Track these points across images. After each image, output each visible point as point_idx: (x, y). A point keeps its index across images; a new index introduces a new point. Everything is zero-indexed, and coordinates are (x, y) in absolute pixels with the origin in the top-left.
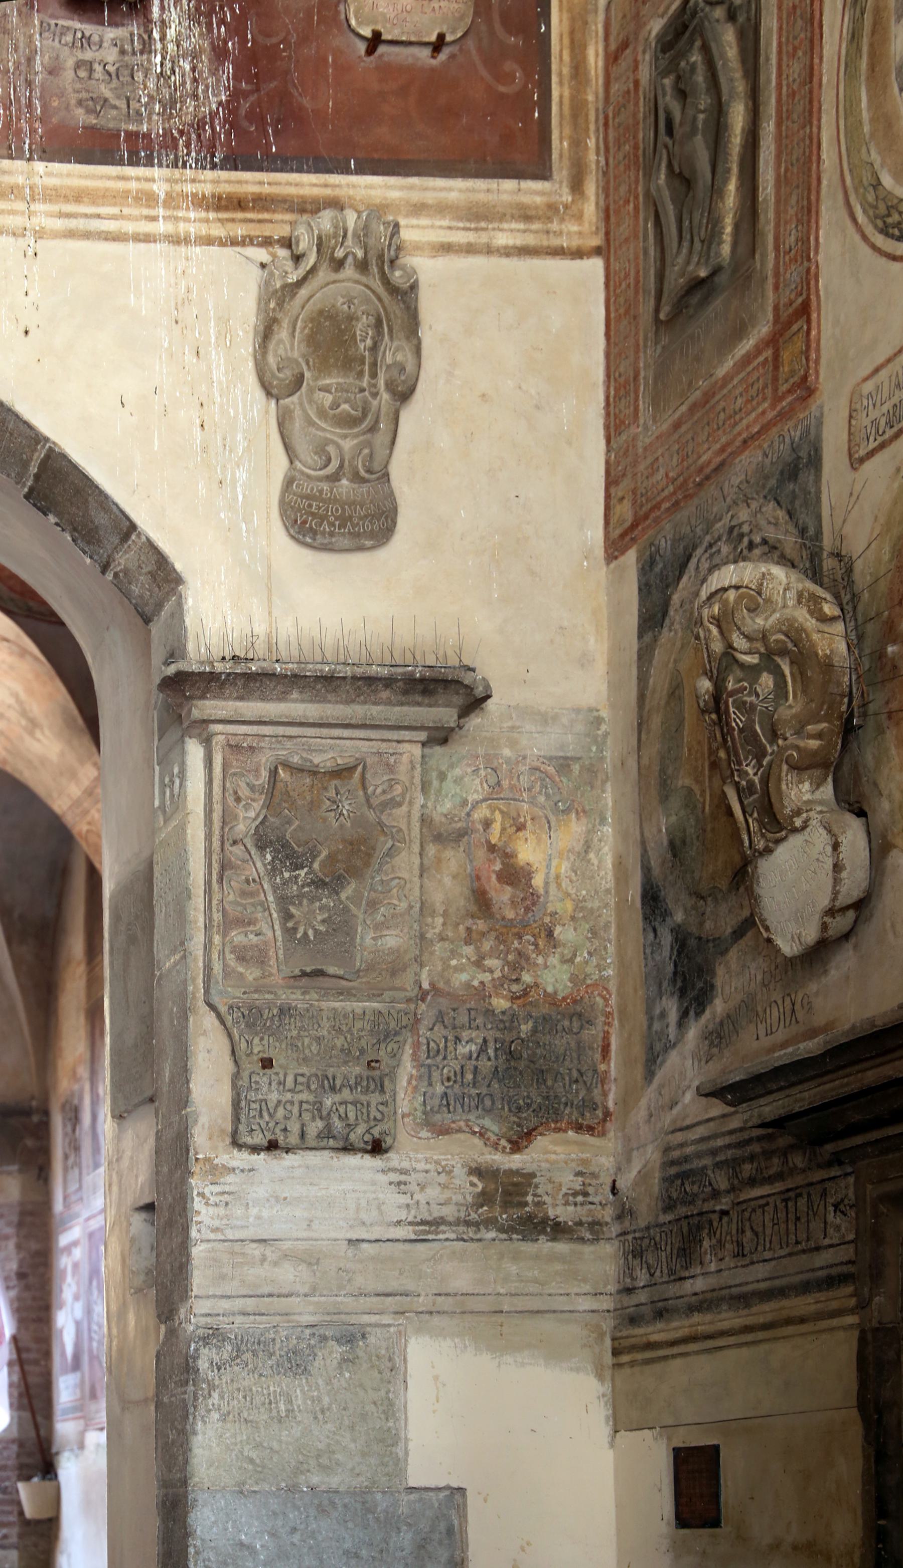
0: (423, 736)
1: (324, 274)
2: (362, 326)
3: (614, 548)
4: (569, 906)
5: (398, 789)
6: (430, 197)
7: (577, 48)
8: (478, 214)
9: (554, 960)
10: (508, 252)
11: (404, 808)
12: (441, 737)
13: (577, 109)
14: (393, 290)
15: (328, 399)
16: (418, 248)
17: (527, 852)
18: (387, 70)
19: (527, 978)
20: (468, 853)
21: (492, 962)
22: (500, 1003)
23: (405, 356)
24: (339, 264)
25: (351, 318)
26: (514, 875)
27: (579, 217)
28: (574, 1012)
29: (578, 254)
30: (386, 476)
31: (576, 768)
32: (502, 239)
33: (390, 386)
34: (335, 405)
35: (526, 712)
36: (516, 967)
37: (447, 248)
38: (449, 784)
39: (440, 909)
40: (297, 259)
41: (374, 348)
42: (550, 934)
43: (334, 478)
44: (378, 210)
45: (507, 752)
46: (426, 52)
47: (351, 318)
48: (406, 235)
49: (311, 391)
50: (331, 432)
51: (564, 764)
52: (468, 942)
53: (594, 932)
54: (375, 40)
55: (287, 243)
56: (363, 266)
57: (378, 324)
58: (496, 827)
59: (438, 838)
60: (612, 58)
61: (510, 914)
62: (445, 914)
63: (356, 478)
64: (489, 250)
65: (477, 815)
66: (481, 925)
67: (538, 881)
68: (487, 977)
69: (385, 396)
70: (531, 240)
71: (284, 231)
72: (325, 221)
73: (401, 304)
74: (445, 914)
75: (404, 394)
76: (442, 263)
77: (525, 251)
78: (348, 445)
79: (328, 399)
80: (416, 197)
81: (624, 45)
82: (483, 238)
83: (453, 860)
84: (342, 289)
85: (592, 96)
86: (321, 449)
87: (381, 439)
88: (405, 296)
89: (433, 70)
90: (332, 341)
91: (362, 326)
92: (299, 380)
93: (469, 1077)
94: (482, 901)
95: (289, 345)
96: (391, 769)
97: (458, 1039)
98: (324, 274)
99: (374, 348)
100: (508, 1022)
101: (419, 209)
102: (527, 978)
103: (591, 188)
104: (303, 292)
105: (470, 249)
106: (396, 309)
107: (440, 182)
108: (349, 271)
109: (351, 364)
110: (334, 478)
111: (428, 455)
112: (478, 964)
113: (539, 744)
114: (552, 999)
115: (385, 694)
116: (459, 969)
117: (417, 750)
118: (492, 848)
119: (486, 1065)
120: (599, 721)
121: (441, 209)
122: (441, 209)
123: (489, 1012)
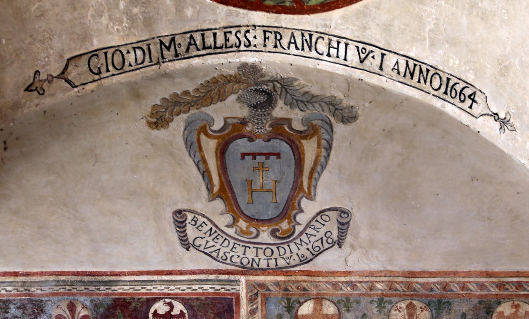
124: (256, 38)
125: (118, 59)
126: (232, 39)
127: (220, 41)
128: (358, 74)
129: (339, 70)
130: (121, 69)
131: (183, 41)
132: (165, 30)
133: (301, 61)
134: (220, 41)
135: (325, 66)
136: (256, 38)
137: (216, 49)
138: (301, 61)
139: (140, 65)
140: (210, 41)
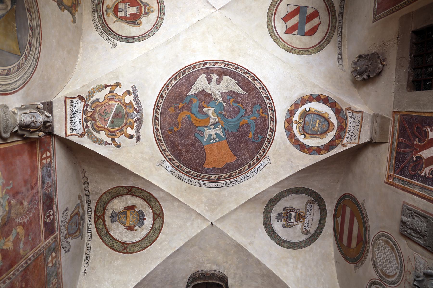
124: (90, 214)
125: (87, 187)
126: (89, 209)
127: (89, 207)
128: (86, 235)
129: (86, 231)
130: (85, 187)
131: (89, 200)
132: (91, 197)
133: (87, 223)
134: (89, 207)
135: (87, 228)
136: (90, 214)
137: (88, 206)
138: (87, 223)
139: (85, 191)
140: (89, 205)
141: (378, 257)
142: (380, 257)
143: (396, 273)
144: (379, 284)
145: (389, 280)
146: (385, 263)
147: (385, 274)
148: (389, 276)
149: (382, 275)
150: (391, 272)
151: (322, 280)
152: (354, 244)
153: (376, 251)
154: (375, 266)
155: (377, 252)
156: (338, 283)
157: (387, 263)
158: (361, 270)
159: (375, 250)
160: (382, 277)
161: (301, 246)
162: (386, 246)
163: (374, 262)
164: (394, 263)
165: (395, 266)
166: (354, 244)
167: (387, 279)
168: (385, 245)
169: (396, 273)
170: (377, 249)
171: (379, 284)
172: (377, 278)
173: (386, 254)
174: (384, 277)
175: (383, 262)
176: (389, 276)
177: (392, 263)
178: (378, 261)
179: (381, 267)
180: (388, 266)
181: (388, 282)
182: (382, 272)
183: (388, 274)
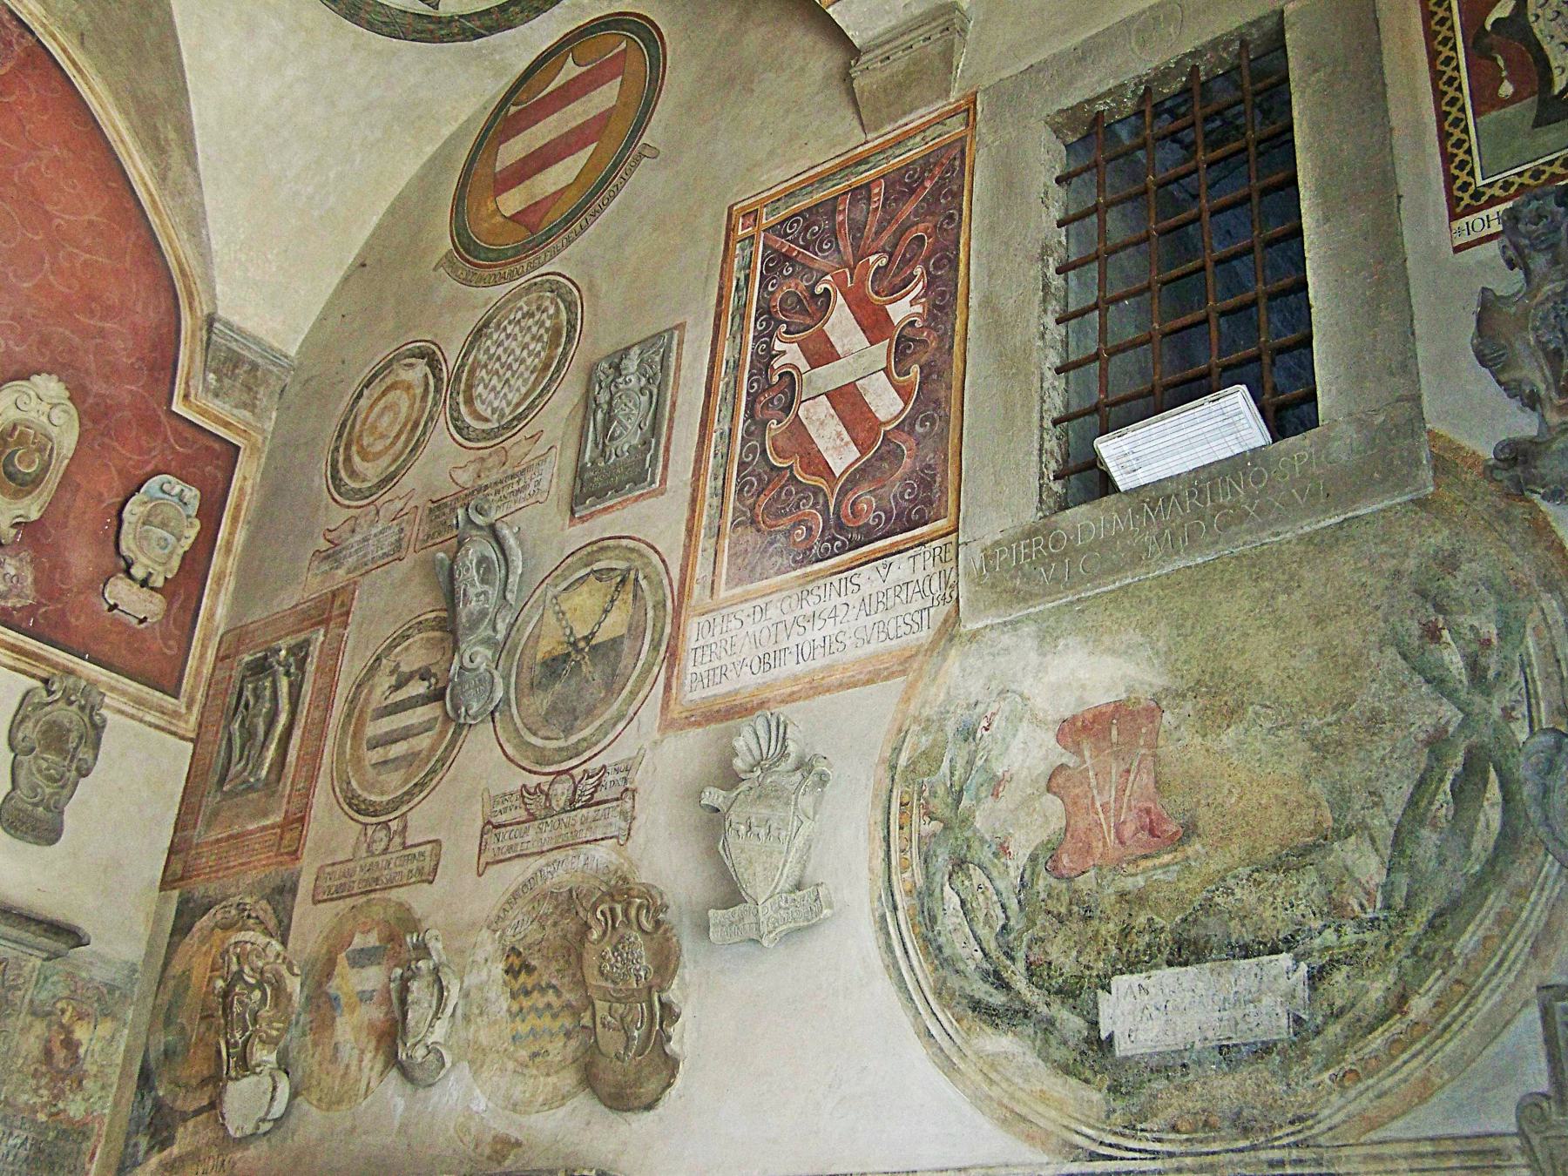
0: (45, 955)
1: (61, 704)
2: (74, 736)
3: (166, 884)
4: (95, 1068)
5: (21, 980)
6: (119, 685)
7: (204, 647)
8: (139, 702)
9: (79, 1098)
10: (150, 725)
11: (20, 993)
12: (54, 956)
13: (198, 673)
14: (94, 725)
15: (45, 765)
16: (108, 707)
17: (81, 1033)
18: (116, 622)
19: (61, 1105)
20: (49, 1026)
21: (44, 1092)
22: (42, 1117)
23: (89, 756)
24: (71, 703)
25: (69, 731)
26: (70, 1044)
27: (187, 722)
28: (81, 1131)
29: (183, 738)
30: (62, 813)
31: (117, 993)
32: (148, 718)
33: (78, 769)
34: (48, 769)
35: (101, 957)
36: (56, 1097)
37: (122, 712)
38: (48, 985)
39: (24, 1053)
40: (50, 693)
41: (76, 749)
42: (80, 1082)
43: (36, 805)
44: (93, 683)
45: (84, 974)
46: (135, 621)
47: (69, 731)
48: (106, 700)
49: (36, 757)
50: (39, 779)
51: (112, 989)
52: (34, 1076)
53: (103, 1088)
54: (115, 606)
55: (46, 681)
56: (82, 708)
57: (81, 738)
58: (68, 1014)
59: (34, 1013)
60: (220, 659)
61: (62, 1066)
62: (26, 1058)
63: (47, 809)
64: (141, 721)
65: (59, 1005)
66: (44, 1069)
67: (82, 1051)
68: (39, 1100)
69: (74, 773)
70: (162, 723)
71: (44, 675)
72: (71, 681)
73: (95, 732)
74: (26, 1058)
75: (83, 773)
76: (118, 717)
77: (157, 727)
78: (48, 791)
79: (45, 765)
80: (113, 683)
81: (227, 657)
82: (140, 714)
83: (39, 1027)
84: (68, 715)
85: (206, 670)
86: (34, 788)
87: (66, 792)
88: (98, 728)
89: (138, 631)
90: (55, 737)
91: (74, 736)
92: (33, 750)
93: (11, 1158)
94: (48, 1053)
95: (29, 730)
96: (20, 968)
97: (11, 1134)
98: (61, 704)
99: (76, 749)
100: (43, 1129)
101: (112, 689)
102: (61, 1105)
103: (196, 709)
104: (48, 709)
105: (132, 717)
106: (92, 733)
107: (127, 681)
108: (74, 708)
109: (61, 751)
110: (36, 805)
111: (85, 808)
112: (36, 1091)
113: (100, 974)
114: (70, 1120)
115: (33, 928)
116: (24, 1092)
117: (39, 962)
118: (62, 1026)
119: (23, 1153)
120: (135, 971)
121: (124, 693)
122: (124, 693)
123: (34, 1121)
141: (505, 329)
142: (508, 336)
143: (487, 420)
144: (438, 379)
145: (463, 408)
146: (497, 365)
147: (470, 387)
148: (469, 401)
149: (465, 375)
150: (483, 402)
151: (332, 175)
152: (512, 201)
153: (521, 308)
154: (479, 333)
155: (519, 315)
156: (375, 220)
157: (501, 372)
158: (448, 286)
159: (521, 303)
160: (458, 378)
161: (362, 14)
162: (545, 338)
163: (486, 325)
164: (510, 396)
165: (504, 403)
166: (512, 201)
167: (461, 399)
168: (547, 330)
169: (487, 420)
170: (525, 309)
171: (438, 379)
172: (451, 364)
173: (525, 353)
174: (462, 386)
175: (499, 359)
176: (469, 401)
177: (506, 389)
178: (495, 337)
179: (483, 358)
180: (495, 381)
181: (455, 408)
182: (472, 372)
183: (475, 393)
